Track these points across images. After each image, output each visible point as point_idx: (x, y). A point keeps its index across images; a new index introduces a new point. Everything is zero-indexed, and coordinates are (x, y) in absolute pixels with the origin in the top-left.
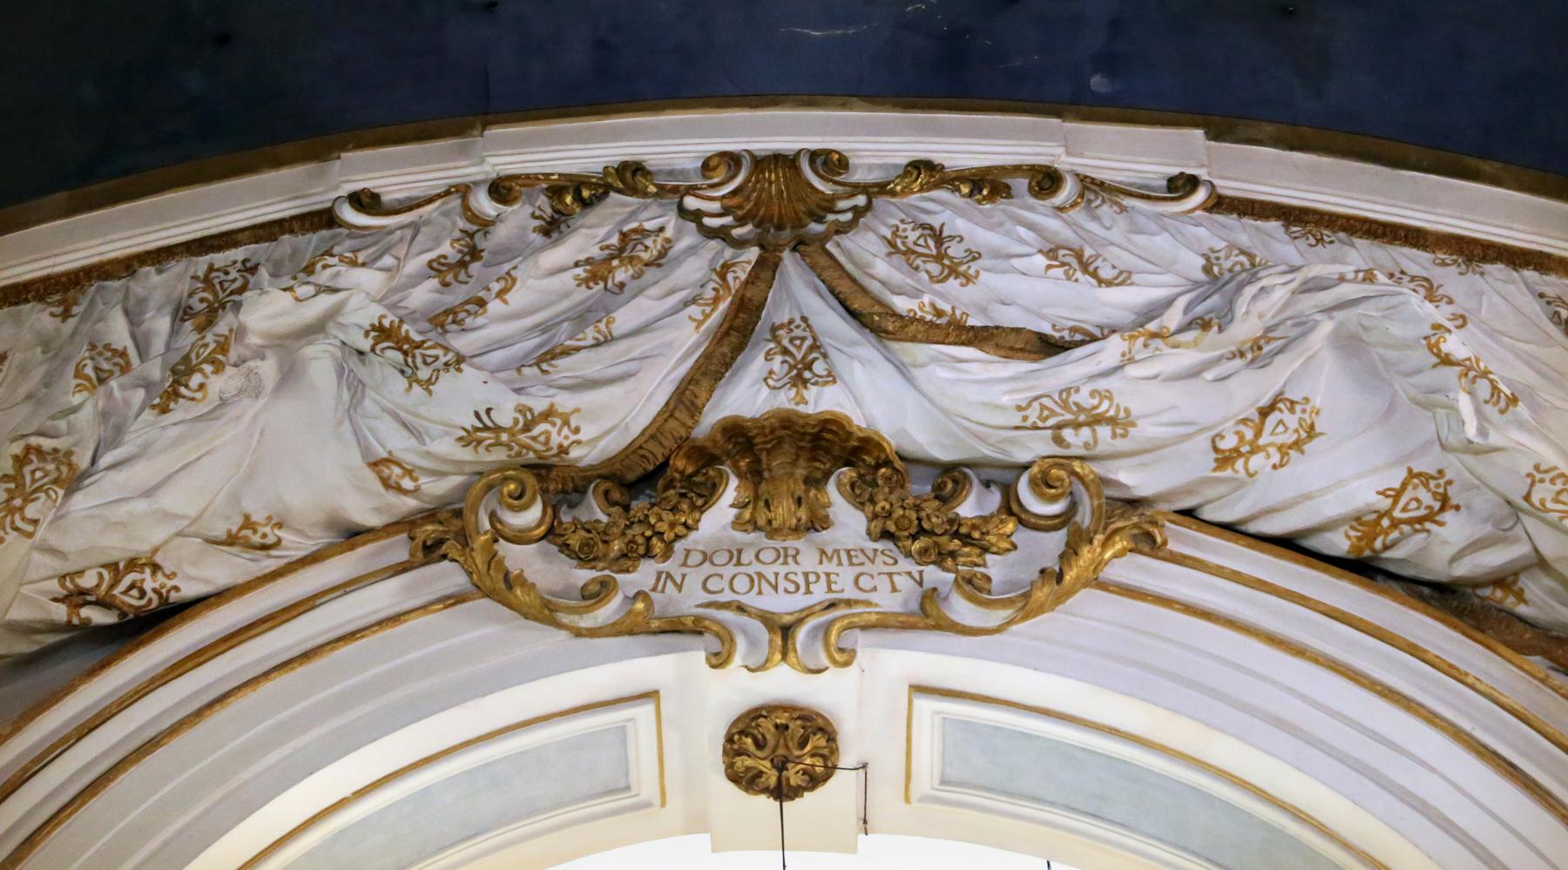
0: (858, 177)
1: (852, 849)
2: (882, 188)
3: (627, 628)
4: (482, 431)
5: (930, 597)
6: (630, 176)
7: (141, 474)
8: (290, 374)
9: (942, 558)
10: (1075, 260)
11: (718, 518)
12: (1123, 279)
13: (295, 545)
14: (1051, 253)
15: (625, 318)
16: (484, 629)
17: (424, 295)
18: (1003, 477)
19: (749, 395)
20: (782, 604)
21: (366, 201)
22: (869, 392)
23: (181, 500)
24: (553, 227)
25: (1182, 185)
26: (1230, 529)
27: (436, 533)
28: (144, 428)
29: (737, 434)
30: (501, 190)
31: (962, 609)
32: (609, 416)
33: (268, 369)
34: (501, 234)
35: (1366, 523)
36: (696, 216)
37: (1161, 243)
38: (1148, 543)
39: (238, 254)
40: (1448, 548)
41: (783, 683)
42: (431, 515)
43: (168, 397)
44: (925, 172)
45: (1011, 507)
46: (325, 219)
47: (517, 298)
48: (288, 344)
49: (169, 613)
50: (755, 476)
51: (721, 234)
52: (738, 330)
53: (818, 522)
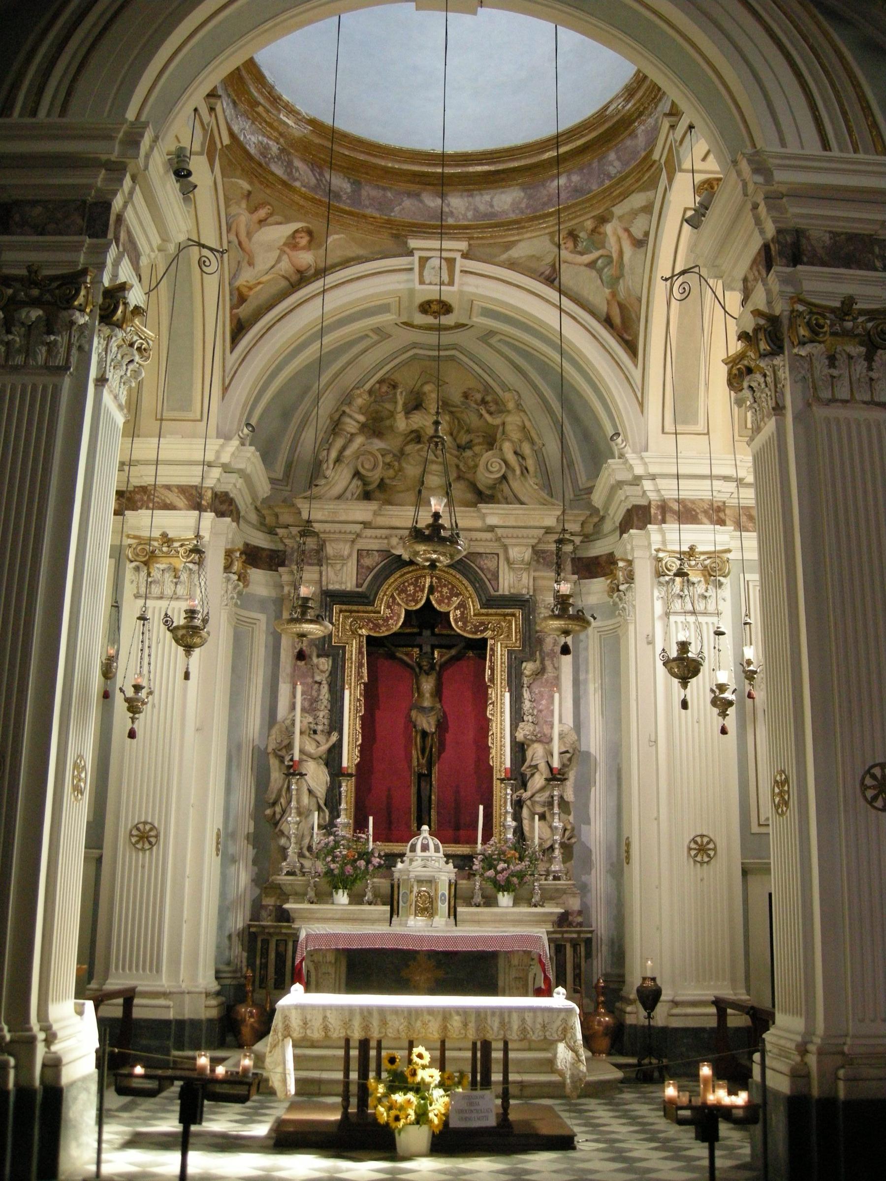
1: (475, 13)
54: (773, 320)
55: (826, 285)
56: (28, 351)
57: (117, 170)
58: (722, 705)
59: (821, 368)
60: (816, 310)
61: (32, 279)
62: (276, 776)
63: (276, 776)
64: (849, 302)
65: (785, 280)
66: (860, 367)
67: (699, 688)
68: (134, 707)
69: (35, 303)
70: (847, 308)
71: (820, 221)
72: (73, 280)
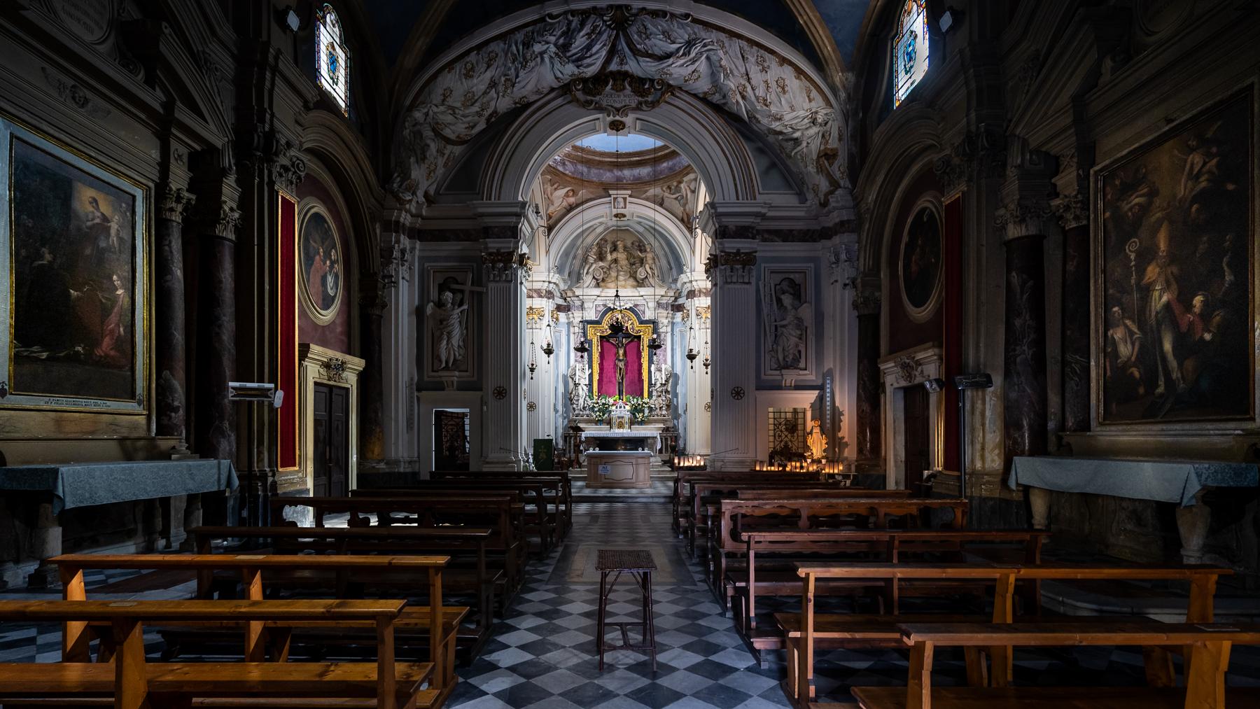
0: (634, 11)
2: (636, 15)
3: (595, 109)
4: (573, 75)
5: (640, 103)
6: (595, 8)
7: (522, 84)
8: (542, 59)
9: (642, 96)
10: (667, 35)
11: (609, 86)
12: (674, 43)
13: (545, 91)
14: (663, 33)
15: (594, 50)
16: (572, 109)
17: (561, 41)
18: (652, 81)
19: (613, 67)
20: (618, 105)
21: (551, 16)
22: (632, 66)
23: (529, 87)
24: (582, 24)
25: (687, 16)
26: (686, 92)
27: (565, 89)
28: (522, 73)
29: (611, 72)
30: (573, 13)
31: (644, 107)
32: (590, 71)
33: (539, 59)
34: (574, 24)
35: (705, 93)
36: (605, 22)
37: (681, 31)
38: (673, 94)
39: (530, 28)
40: (716, 98)
41: (617, 118)
42: (565, 85)
43: (524, 67)
44: (644, 9)
45: (653, 86)
46: (542, 20)
47: (577, 43)
48: (542, 54)
49: (529, 105)
50: (614, 80)
51: (609, 26)
52: (612, 52)
53: (624, 88)
54: (715, 256)
55: (732, 245)
56: (500, 276)
57: (519, 215)
58: (706, 366)
59: (728, 273)
60: (728, 254)
61: (498, 253)
62: (571, 385)
63: (571, 385)
64: (738, 250)
65: (720, 243)
66: (740, 272)
67: (698, 362)
68: (532, 370)
69: (500, 261)
70: (738, 253)
71: (732, 222)
72: (511, 254)
